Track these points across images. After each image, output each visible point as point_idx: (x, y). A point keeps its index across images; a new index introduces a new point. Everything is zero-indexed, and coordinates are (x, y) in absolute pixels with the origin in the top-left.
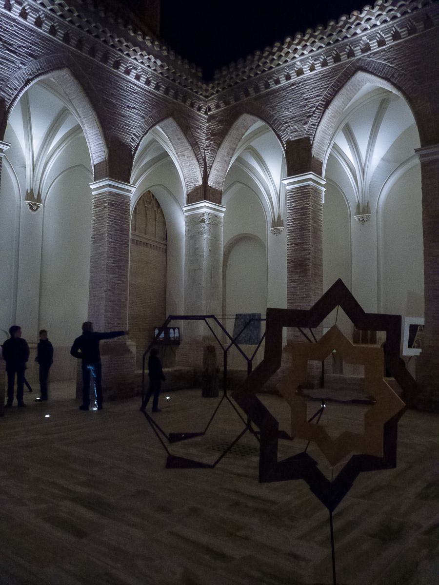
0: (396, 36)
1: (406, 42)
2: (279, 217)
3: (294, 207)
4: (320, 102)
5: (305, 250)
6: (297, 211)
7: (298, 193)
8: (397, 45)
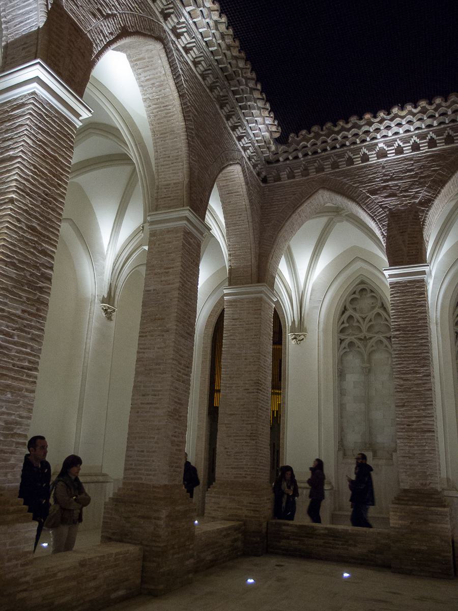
3: (40, 141)
4: (118, 14)
5: (44, 253)
6: (44, 156)
7: (55, 122)
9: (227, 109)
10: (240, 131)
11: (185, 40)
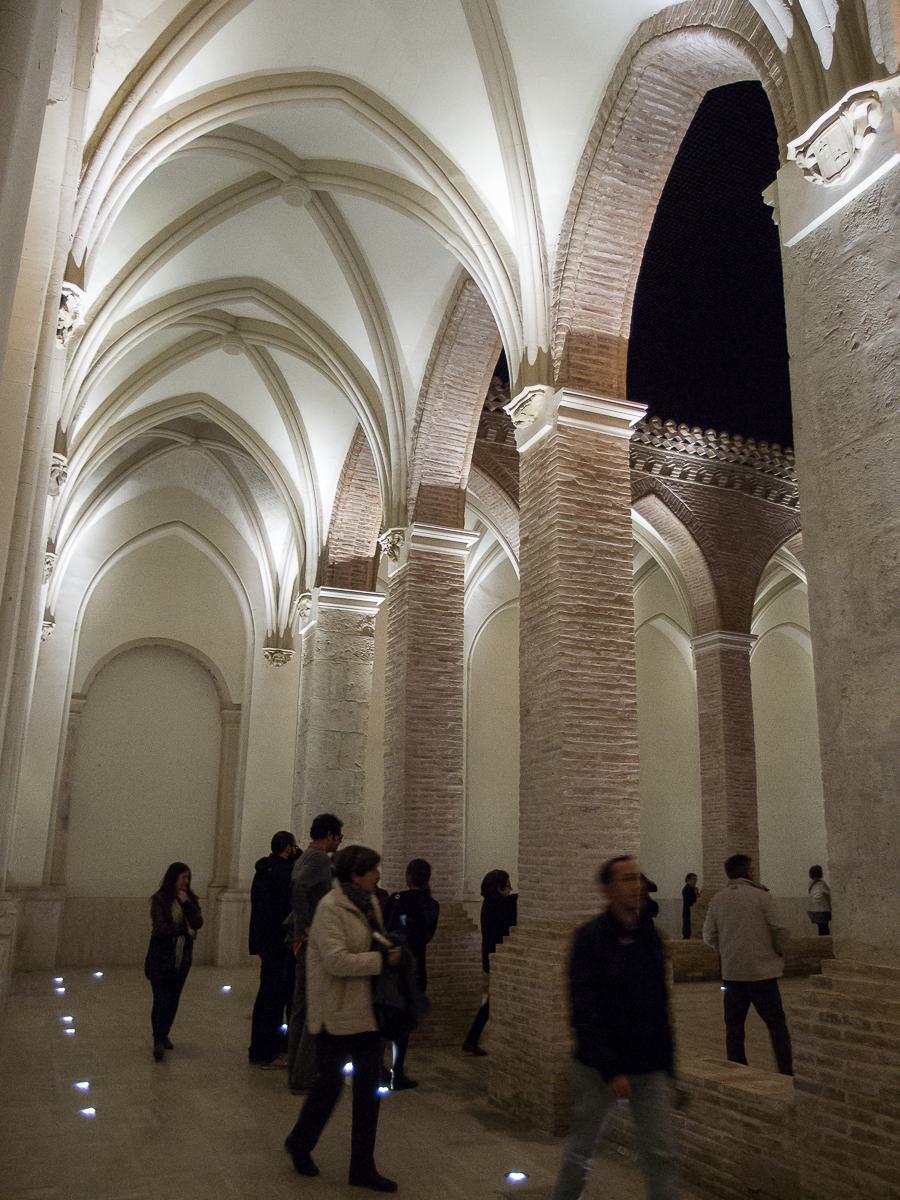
0: (699, 478)
1: (706, 489)
2: (288, 630)
8: (697, 487)
9: (759, 490)
10: (788, 498)
11: (677, 472)
